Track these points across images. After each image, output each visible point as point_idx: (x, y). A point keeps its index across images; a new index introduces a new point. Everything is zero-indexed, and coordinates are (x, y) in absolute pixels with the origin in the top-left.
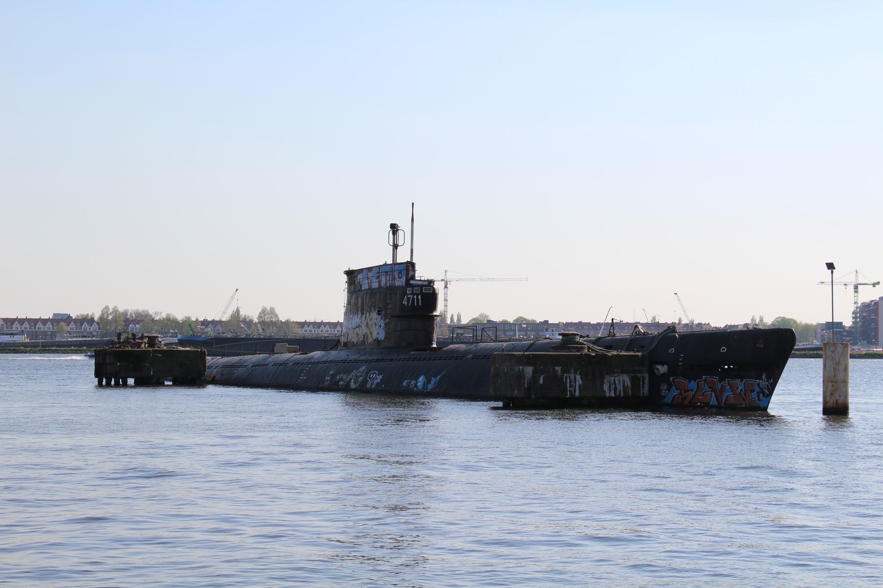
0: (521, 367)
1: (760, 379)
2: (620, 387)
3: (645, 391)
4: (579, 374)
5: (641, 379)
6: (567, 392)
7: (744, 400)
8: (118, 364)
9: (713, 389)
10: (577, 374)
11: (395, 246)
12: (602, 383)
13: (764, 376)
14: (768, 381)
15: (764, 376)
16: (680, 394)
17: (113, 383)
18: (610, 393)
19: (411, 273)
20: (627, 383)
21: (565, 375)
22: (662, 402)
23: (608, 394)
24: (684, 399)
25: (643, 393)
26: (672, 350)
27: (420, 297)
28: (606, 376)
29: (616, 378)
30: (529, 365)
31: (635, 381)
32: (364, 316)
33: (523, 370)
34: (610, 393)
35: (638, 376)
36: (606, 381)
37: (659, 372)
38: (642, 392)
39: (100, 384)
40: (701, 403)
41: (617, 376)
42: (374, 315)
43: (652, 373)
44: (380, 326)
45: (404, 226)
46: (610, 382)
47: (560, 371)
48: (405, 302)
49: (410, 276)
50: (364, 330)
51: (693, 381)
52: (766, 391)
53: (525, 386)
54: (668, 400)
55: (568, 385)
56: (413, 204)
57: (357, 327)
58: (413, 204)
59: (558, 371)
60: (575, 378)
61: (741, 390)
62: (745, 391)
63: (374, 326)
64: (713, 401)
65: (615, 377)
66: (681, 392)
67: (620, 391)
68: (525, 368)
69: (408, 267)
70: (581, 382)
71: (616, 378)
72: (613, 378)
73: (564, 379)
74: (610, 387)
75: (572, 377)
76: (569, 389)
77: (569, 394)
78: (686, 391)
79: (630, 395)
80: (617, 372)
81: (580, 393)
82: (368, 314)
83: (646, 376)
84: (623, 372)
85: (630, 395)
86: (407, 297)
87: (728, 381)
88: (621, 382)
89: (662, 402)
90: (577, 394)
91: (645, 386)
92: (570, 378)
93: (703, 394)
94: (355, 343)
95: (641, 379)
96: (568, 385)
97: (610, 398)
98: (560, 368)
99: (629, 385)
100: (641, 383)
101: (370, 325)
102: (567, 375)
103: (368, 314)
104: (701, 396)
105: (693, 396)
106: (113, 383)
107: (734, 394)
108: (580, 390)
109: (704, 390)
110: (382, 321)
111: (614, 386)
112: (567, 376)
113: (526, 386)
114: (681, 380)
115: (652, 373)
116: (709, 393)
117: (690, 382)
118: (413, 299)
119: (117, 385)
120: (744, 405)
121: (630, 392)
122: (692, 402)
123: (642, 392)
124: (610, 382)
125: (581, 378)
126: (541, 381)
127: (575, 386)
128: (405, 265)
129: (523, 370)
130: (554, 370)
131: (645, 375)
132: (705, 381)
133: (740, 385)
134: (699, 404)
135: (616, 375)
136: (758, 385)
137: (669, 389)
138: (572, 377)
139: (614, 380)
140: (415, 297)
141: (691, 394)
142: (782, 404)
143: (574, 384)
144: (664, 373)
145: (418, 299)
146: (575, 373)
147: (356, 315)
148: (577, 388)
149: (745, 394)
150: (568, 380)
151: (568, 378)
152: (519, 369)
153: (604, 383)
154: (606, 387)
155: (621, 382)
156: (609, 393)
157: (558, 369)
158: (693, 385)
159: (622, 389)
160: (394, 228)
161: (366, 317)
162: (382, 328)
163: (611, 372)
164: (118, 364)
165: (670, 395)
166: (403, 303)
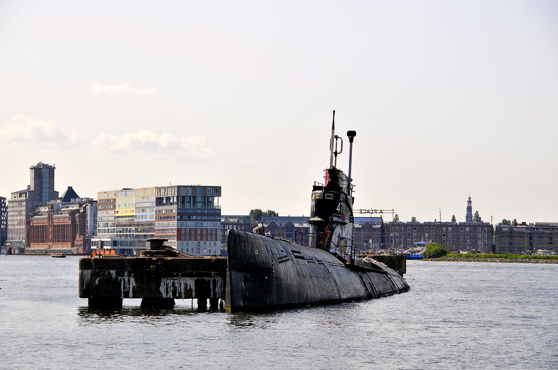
4: (133, 277)
5: (212, 283)
6: (121, 294)
10: (131, 277)
12: (159, 285)
18: (167, 295)
20: (190, 286)
21: (119, 277)
28: (163, 279)
34: (167, 295)
35: (205, 280)
36: (162, 284)
41: (177, 279)
46: (167, 285)
48: (338, 208)
53: (84, 288)
55: (122, 286)
56: (334, 112)
58: (334, 112)
59: (112, 273)
60: (129, 281)
68: (84, 271)
70: (134, 285)
72: (172, 281)
75: (126, 279)
76: (122, 290)
80: (177, 276)
84: (184, 276)
86: (340, 204)
92: (124, 281)
95: (212, 283)
96: (122, 286)
98: (115, 271)
100: (211, 286)
102: (121, 277)
108: (133, 292)
111: (172, 288)
112: (121, 279)
113: (85, 288)
124: (167, 285)
126: (97, 282)
127: (129, 288)
130: (109, 273)
131: (217, 279)
135: (175, 278)
138: (126, 279)
139: (174, 283)
142: (124, 304)
143: (128, 286)
146: (129, 276)
151: (122, 280)
153: (160, 285)
154: (162, 289)
157: (113, 272)
159: (183, 291)
163: (168, 275)
166: (337, 209)
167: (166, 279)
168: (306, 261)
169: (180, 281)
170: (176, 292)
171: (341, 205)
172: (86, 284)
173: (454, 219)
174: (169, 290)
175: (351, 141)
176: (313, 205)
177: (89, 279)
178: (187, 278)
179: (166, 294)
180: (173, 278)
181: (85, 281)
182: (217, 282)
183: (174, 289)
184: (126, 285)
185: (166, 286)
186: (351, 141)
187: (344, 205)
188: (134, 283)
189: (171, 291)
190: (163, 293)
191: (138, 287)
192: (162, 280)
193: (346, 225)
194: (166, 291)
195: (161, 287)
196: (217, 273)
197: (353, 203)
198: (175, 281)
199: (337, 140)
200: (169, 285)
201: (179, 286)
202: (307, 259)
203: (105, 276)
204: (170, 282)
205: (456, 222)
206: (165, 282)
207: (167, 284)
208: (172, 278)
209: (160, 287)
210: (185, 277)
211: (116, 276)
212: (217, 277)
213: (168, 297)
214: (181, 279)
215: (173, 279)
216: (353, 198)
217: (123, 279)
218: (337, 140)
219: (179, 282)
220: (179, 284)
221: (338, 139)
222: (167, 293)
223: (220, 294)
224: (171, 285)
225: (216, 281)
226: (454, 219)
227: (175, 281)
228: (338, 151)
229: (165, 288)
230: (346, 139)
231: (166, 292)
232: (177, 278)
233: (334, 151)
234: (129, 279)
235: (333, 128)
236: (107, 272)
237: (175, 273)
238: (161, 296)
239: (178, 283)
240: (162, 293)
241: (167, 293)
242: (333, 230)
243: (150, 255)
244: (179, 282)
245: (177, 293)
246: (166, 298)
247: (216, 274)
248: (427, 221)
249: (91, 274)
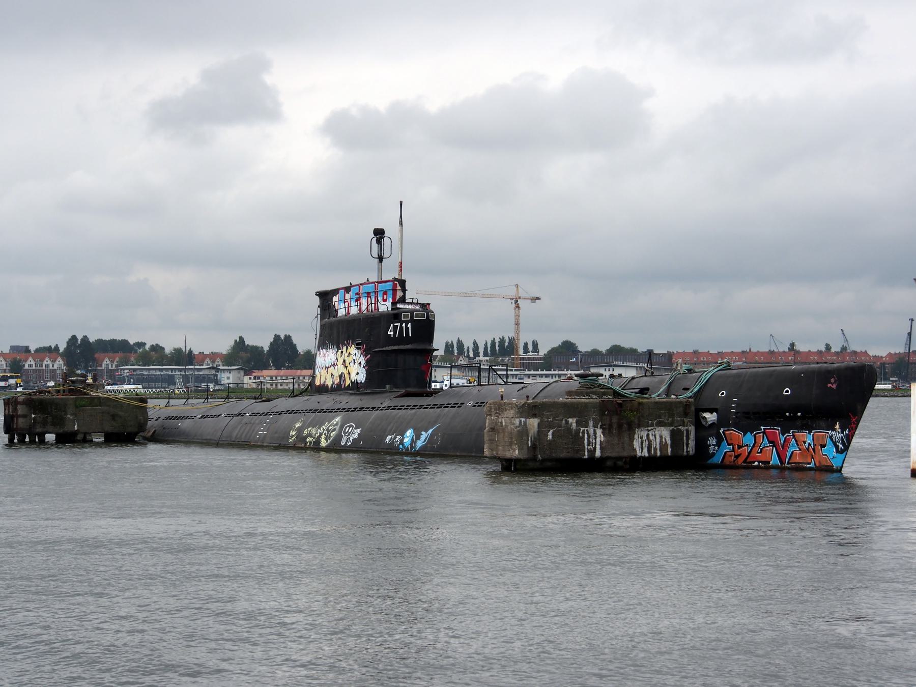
0: (523, 420)
1: (834, 430)
2: (656, 444)
3: (690, 447)
5: (685, 432)
7: (813, 458)
8: (33, 416)
9: (774, 443)
11: (381, 259)
12: (632, 439)
13: (837, 427)
14: (842, 432)
15: (837, 427)
16: (733, 450)
17: (27, 439)
19: (399, 294)
20: (665, 439)
21: (582, 429)
22: (710, 461)
23: (639, 454)
24: (737, 457)
25: (687, 452)
26: (723, 393)
27: (409, 325)
29: (650, 433)
30: (534, 416)
31: (676, 436)
32: (340, 351)
33: (525, 423)
36: (636, 436)
37: (707, 422)
38: (685, 450)
39: (11, 440)
40: (759, 462)
41: (652, 429)
42: (353, 350)
43: (699, 423)
44: (360, 363)
45: (391, 231)
46: (641, 438)
47: (574, 425)
48: (391, 332)
49: (398, 297)
50: (341, 369)
51: (749, 433)
52: (841, 446)
54: (718, 459)
55: (586, 441)
56: (401, 203)
57: (332, 365)
58: (401, 203)
59: (571, 423)
60: (595, 434)
61: (810, 444)
62: (815, 445)
63: (352, 364)
64: (775, 460)
65: (649, 431)
66: (733, 448)
67: (655, 449)
68: (528, 420)
69: (395, 285)
70: (602, 439)
71: (650, 433)
72: (646, 433)
73: (581, 434)
75: (591, 431)
76: (586, 447)
77: (586, 453)
78: (740, 447)
79: (669, 454)
80: (652, 425)
81: (601, 452)
82: (345, 348)
83: (692, 429)
85: (669, 454)
86: (393, 325)
87: (793, 432)
88: (658, 437)
89: (710, 461)
90: (598, 453)
91: (690, 442)
92: (588, 433)
93: (762, 449)
94: (329, 387)
96: (586, 441)
97: (643, 458)
99: (669, 442)
100: (685, 438)
101: (347, 362)
103: (345, 348)
104: (758, 453)
105: (749, 453)
106: (27, 439)
107: (800, 450)
108: (601, 448)
109: (763, 446)
110: (362, 357)
111: (647, 443)
112: (584, 431)
114: (733, 433)
115: (699, 423)
116: (769, 448)
117: (744, 435)
118: (401, 327)
119: (32, 442)
120: (812, 465)
121: (669, 450)
122: (748, 460)
123: (685, 450)
125: (603, 433)
126: (550, 437)
127: (596, 443)
128: (391, 283)
129: (525, 423)
130: (567, 422)
131: (690, 428)
132: (764, 433)
133: (808, 438)
134: (756, 463)
135: (650, 428)
136: (831, 437)
137: (719, 444)
138: (591, 431)
139: (648, 435)
140: (404, 325)
141: (746, 450)
144: (713, 424)
145: (407, 329)
146: (595, 426)
147: (331, 350)
148: (598, 447)
149: (814, 449)
150: (586, 436)
151: (586, 432)
152: (520, 421)
154: (636, 444)
155: (658, 437)
156: (641, 452)
158: (749, 438)
159: (658, 447)
160: (379, 234)
161: (342, 352)
162: (362, 366)
164: (33, 416)
165: (720, 452)
166: (389, 333)
172: (531, 438)
173: (828, 347)
177: (536, 432)
178: (662, 428)
181: (530, 435)
184: (591, 440)
188: (602, 435)
190: (638, 449)
191: (607, 441)
195: (635, 441)
203: (560, 426)
204: (644, 434)
205: (580, 349)
210: (660, 426)
211: (577, 426)
215: (647, 430)
217: (587, 430)
226: (828, 347)
229: (640, 443)
232: (652, 428)
234: (595, 430)
235: (401, 224)
236: (564, 422)
238: (635, 454)
246: (641, 457)
247: (689, 421)
248: (548, 350)
249: (539, 424)
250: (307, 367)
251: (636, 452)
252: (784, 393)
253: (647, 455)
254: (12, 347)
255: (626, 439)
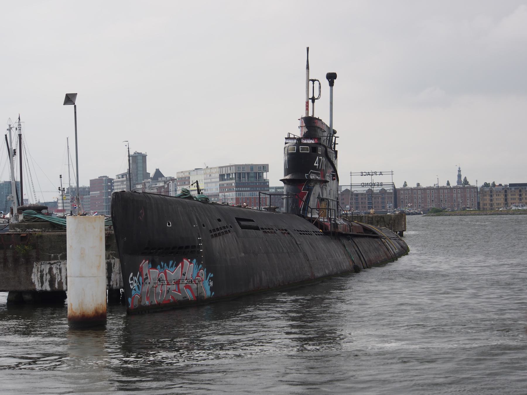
12: (29, 273)
18: (42, 286)
23: (38, 287)
28: (35, 263)
34: (42, 286)
36: (35, 270)
41: (55, 263)
46: (41, 271)
48: (316, 163)
56: (308, 49)
58: (308, 49)
71: (54, 266)
72: (48, 266)
74: (42, 277)
80: (56, 258)
86: (319, 158)
97: (44, 293)
111: (48, 277)
135: (52, 262)
139: (51, 269)
154: (35, 278)
166: (315, 164)
167: (40, 263)
168: (261, 232)
169: (60, 265)
170: (55, 282)
171: (319, 160)
174: (44, 280)
175: (331, 84)
176: (286, 160)
179: (40, 285)
180: (50, 262)
182: (113, 265)
183: (51, 277)
185: (39, 273)
186: (331, 84)
187: (323, 159)
189: (47, 281)
190: (36, 283)
192: (35, 266)
193: (327, 184)
194: (39, 280)
195: (33, 275)
196: (113, 252)
197: (336, 157)
198: (52, 266)
199: (313, 84)
200: (44, 272)
201: (59, 273)
202: (262, 229)
204: (46, 268)
206: (38, 268)
207: (41, 270)
208: (48, 262)
209: (31, 275)
212: (113, 258)
213: (44, 289)
214: (60, 262)
215: (49, 263)
216: (336, 152)
218: (313, 84)
219: (58, 268)
220: (58, 270)
221: (315, 82)
222: (42, 283)
223: (118, 282)
224: (47, 271)
225: (111, 264)
227: (52, 266)
228: (316, 97)
229: (39, 276)
230: (325, 83)
231: (40, 282)
232: (55, 261)
233: (311, 96)
235: (308, 67)
237: (52, 255)
238: (33, 287)
239: (57, 268)
240: (34, 283)
241: (42, 283)
242: (310, 190)
243: (21, 230)
244: (58, 268)
245: (57, 282)
247: (112, 254)
250: (428, 191)
251: (35, 286)
252: (171, 226)
253: (49, 289)
254: (91, 181)
255: (23, 273)
